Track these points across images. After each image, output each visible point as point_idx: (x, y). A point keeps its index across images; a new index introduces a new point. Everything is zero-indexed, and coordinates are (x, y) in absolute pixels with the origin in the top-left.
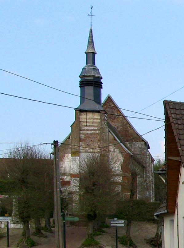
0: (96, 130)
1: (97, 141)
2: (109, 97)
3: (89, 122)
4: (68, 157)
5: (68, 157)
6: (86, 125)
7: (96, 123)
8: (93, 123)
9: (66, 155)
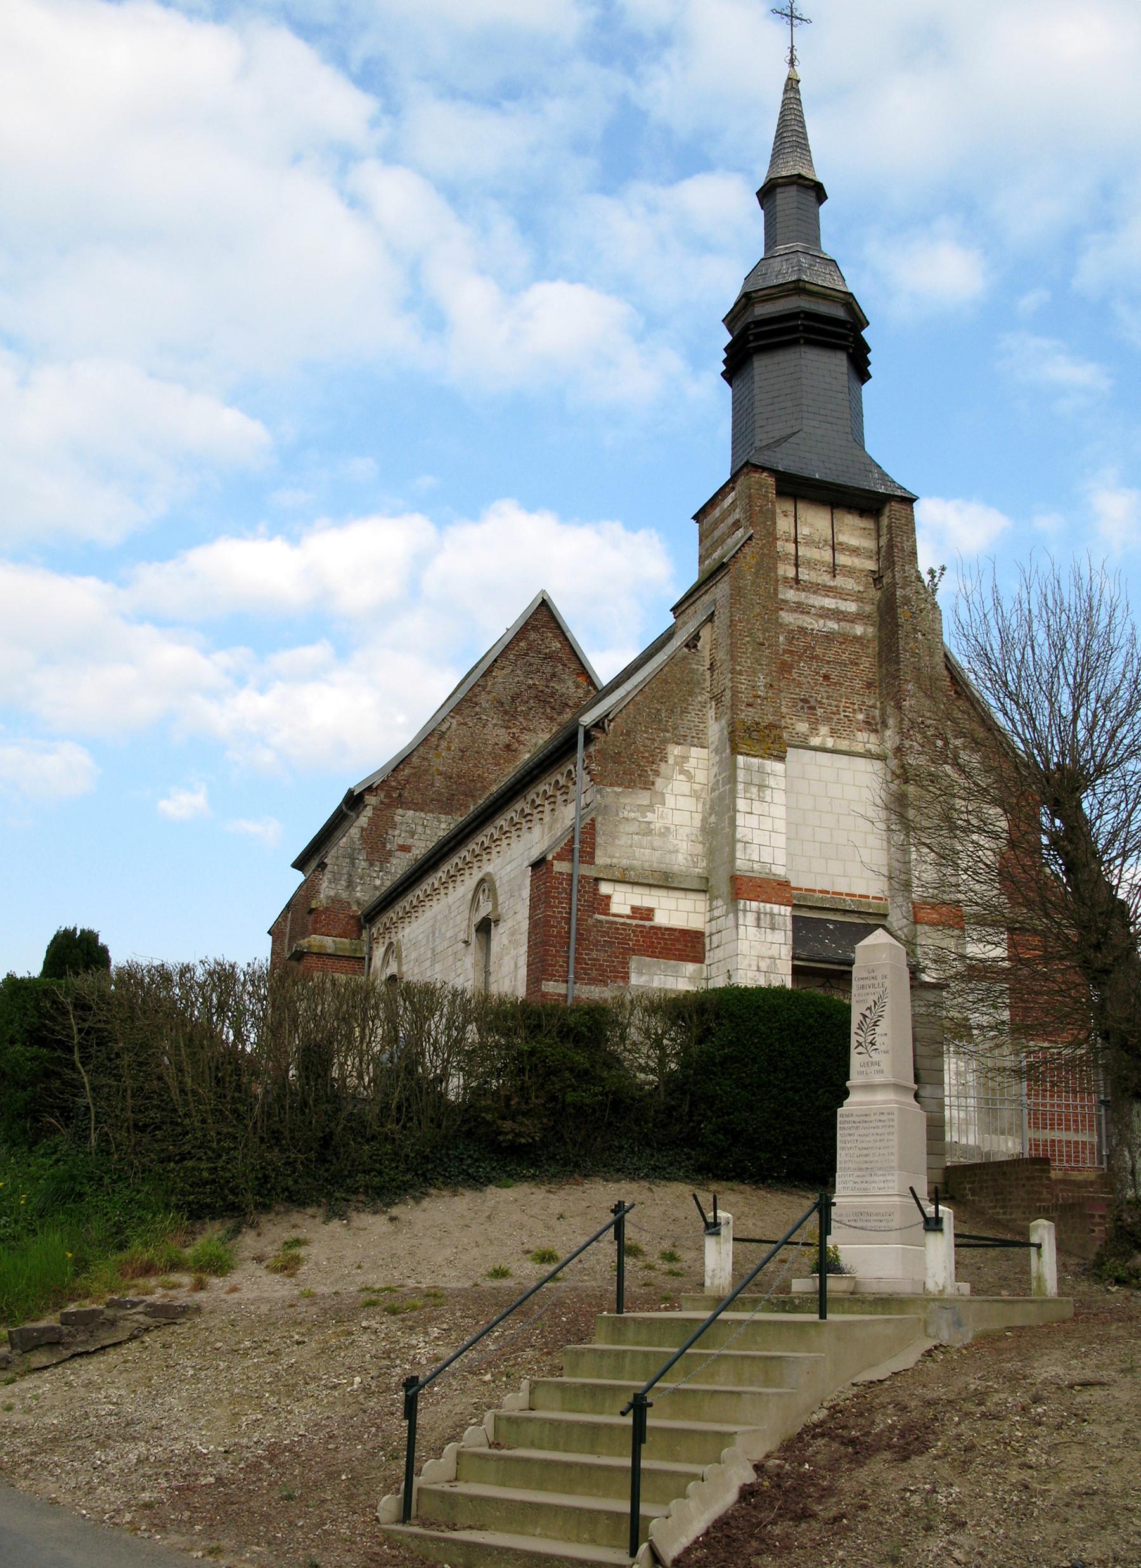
0: (852, 619)
1: (858, 684)
2: (544, 601)
3: (812, 564)
4: (686, 767)
5: (686, 767)
6: (791, 573)
7: (850, 572)
8: (834, 570)
9: (674, 751)
